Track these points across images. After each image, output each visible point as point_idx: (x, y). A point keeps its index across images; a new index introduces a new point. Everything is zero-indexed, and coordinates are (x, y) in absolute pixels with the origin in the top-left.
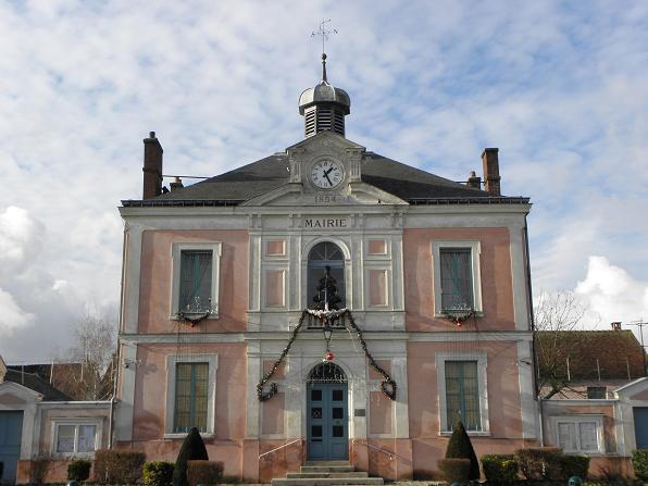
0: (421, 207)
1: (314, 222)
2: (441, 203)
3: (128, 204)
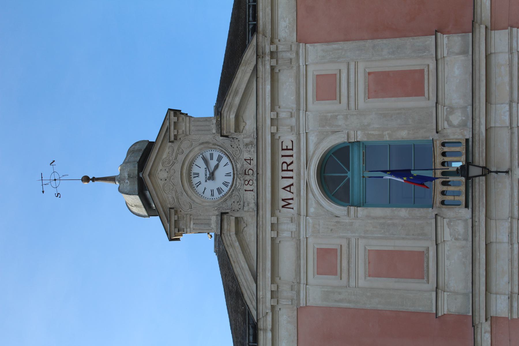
0: (261, 14)
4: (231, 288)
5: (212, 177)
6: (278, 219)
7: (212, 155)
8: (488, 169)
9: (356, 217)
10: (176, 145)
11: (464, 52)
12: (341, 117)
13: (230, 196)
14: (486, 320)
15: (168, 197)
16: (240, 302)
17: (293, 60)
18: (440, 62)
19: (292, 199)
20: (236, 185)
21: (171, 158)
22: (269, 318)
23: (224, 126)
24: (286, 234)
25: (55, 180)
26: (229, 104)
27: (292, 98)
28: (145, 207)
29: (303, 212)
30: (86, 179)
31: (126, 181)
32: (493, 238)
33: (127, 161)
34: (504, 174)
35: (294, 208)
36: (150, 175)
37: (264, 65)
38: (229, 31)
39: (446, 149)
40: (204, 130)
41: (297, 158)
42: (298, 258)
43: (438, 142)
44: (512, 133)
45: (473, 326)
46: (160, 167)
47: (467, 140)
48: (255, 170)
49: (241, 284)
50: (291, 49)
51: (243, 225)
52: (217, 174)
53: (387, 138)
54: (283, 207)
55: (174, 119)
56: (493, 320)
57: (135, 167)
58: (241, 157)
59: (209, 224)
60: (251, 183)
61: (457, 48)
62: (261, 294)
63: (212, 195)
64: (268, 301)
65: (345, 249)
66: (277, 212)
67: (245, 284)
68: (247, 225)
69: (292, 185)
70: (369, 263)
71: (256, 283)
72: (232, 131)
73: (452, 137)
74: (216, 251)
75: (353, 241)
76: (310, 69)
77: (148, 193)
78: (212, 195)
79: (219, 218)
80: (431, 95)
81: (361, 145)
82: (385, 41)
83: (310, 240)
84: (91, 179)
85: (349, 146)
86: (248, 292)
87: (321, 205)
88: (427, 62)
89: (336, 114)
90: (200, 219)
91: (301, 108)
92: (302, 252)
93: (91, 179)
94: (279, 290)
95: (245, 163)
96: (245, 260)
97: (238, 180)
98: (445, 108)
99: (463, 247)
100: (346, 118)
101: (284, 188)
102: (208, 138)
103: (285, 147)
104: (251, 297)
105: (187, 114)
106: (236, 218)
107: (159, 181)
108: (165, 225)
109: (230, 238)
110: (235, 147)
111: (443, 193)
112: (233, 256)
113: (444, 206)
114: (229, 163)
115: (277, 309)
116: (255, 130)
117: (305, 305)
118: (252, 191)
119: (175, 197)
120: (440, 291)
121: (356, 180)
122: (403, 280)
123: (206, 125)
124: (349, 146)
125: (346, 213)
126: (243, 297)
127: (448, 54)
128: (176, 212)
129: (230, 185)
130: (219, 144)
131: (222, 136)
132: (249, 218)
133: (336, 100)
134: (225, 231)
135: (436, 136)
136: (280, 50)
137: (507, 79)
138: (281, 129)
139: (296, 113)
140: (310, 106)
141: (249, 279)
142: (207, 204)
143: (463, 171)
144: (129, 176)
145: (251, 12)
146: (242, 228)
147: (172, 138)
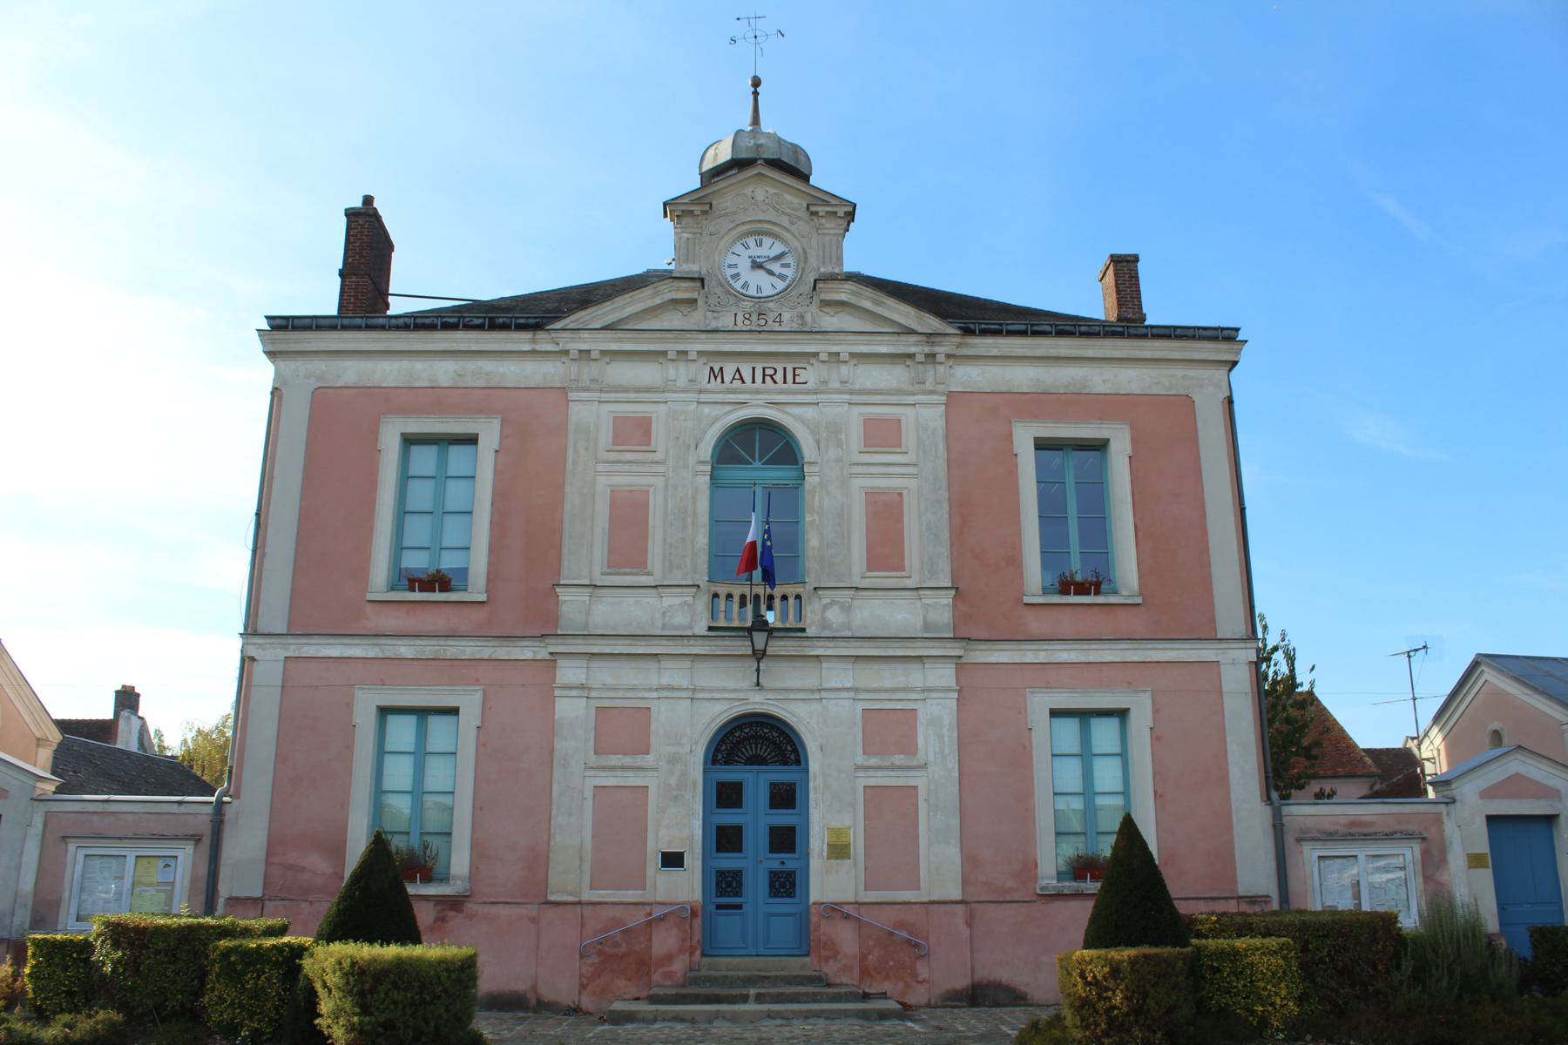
2: (1035, 334)
3: (281, 325)
4: (596, 292)
5: (757, 265)
6: (694, 360)
7: (787, 266)
8: (762, 658)
9: (696, 474)
10: (803, 214)
11: (927, 626)
12: (840, 454)
13: (728, 293)
14: (551, 654)
16: (575, 306)
18: (914, 593)
19: (723, 382)
20: (744, 300)
21: (784, 206)
22: (550, 347)
23: (830, 285)
25: (756, 37)
26: (862, 292)
28: (714, 168)
29: (704, 397)
30: (756, 83)
31: (752, 141)
32: (665, 664)
33: (783, 143)
34: (756, 680)
35: (709, 385)
36: (760, 174)
38: (966, 296)
39: (791, 600)
42: (638, 390)
43: (802, 590)
44: (812, 691)
45: (543, 635)
46: (772, 191)
47: (803, 630)
48: (765, 328)
49: (600, 306)
51: (685, 309)
52: (761, 273)
53: (808, 518)
54: (712, 368)
55: (841, 211)
56: (551, 662)
57: (773, 154)
58: (784, 309)
59: (687, 261)
60: (747, 322)
61: (933, 617)
62: (586, 335)
63: (730, 266)
64: (575, 344)
65: (650, 456)
66: (704, 360)
67: (600, 312)
68: (686, 316)
69: (743, 382)
70: (631, 491)
71: (602, 329)
72: (823, 296)
73: (808, 609)
74: (648, 271)
75: (661, 469)
76: (909, 411)
77: (734, 172)
78: (730, 266)
79: (696, 276)
80: (868, 580)
81: (798, 482)
82: (946, 516)
83: (663, 407)
84: (756, 90)
85: (797, 464)
86: (589, 317)
87: (713, 423)
89: (844, 447)
91: (853, 397)
92: (646, 395)
93: (756, 90)
94: (592, 362)
95: (776, 314)
97: (751, 304)
98: (850, 600)
99: (653, 623)
100: (839, 461)
101: (738, 370)
103: (797, 372)
104: (581, 321)
105: (848, 231)
106: (695, 301)
107: (751, 190)
108: (687, 196)
109: (668, 292)
110: (799, 301)
112: (640, 296)
113: (711, 597)
114: (776, 291)
115: (564, 359)
116: (823, 329)
117: (569, 398)
118: (735, 324)
119: (727, 211)
120: (591, 590)
121: (748, 474)
122: (606, 538)
123: (831, 259)
124: (797, 464)
125: (702, 459)
126: (582, 309)
127: (925, 604)
128: (705, 213)
129: (744, 292)
130: (804, 276)
131: (815, 280)
132: (696, 319)
133: (865, 446)
134: (677, 284)
135: (809, 587)
136: (938, 367)
137: (888, 684)
138: (824, 367)
140: (856, 410)
141: (607, 318)
142: (717, 258)
143: (760, 624)
144: (759, 146)
145: (993, 327)
146: (682, 309)
147: (813, 209)
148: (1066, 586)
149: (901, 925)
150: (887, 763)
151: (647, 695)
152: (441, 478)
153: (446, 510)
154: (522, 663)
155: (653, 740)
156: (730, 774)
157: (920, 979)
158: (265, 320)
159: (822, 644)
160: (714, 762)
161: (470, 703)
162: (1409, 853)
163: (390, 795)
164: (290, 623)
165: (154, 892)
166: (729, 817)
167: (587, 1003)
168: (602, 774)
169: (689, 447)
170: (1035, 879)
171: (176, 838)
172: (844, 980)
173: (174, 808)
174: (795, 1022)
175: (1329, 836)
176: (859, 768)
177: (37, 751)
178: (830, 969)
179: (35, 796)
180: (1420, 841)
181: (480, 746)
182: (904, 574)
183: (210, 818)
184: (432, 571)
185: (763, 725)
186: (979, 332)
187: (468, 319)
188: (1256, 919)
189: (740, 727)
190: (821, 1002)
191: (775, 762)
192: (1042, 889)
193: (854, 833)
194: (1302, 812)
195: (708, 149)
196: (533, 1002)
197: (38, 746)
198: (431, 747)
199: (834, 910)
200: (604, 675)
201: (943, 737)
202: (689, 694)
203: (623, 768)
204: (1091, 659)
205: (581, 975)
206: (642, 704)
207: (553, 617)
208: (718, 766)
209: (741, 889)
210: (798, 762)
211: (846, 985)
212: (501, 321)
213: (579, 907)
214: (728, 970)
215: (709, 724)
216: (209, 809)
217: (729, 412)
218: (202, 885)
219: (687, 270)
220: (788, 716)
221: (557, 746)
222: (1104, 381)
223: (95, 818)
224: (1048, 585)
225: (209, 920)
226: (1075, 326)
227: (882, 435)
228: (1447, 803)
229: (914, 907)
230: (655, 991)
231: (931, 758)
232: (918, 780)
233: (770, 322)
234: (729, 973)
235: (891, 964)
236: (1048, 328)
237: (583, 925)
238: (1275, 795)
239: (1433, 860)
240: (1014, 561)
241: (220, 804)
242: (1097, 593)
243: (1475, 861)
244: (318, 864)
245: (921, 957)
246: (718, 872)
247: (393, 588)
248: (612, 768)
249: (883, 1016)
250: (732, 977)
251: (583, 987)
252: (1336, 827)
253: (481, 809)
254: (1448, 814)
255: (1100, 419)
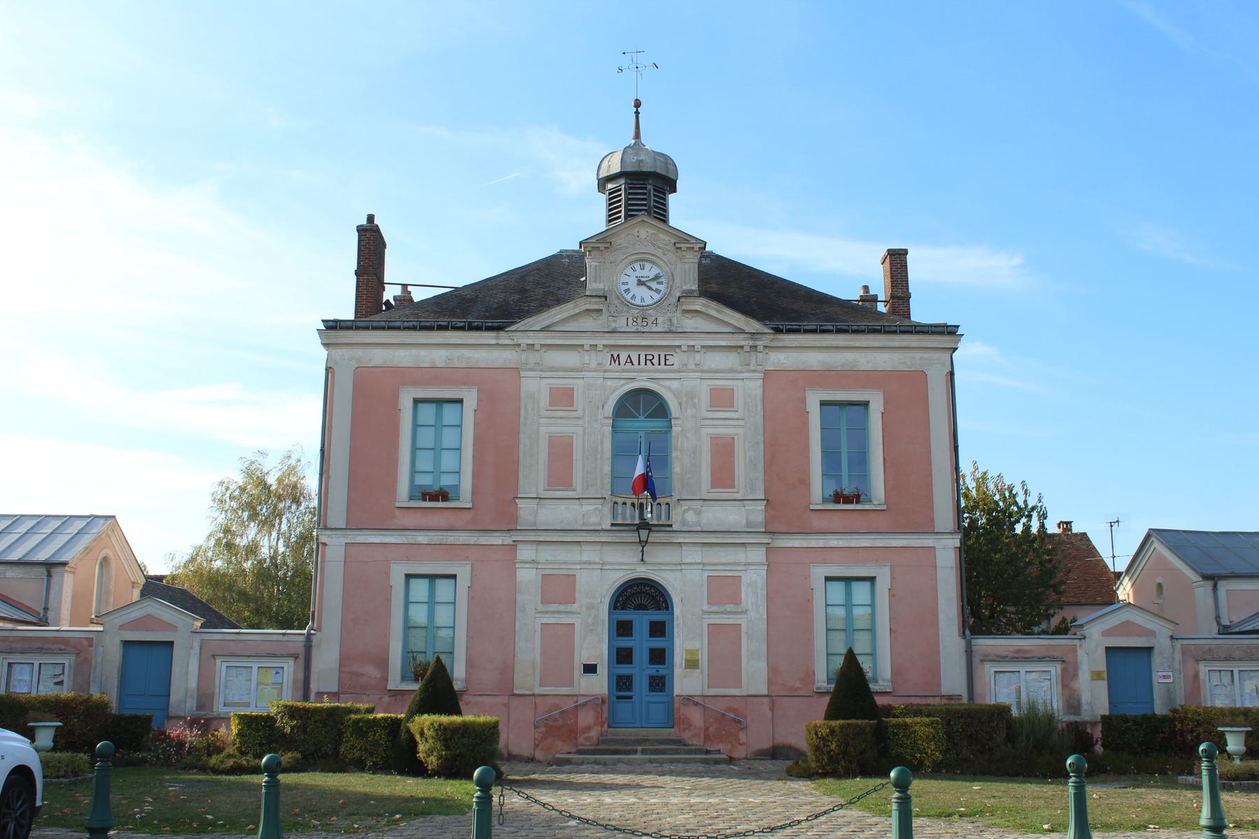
0: (792, 337)
1: (623, 358)
3: (333, 326)
5: (640, 283)
7: (661, 283)
9: (602, 425)
10: (671, 247)
11: (748, 524)
14: (514, 541)
15: (621, 239)
17: (748, 367)
19: (619, 364)
22: (508, 342)
23: (689, 300)
24: (587, 359)
27: (713, 365)
29: (608, 375)
32: (584, 547)
36: (643, 221)
37: (744, 339)
40: (685, 278)
41: (657, 369)
42: (565, 370)
44: (676, 565)
45: (508, 530)
46: (651, 231)
50: (758, 365)
52: (644, 288)
53: (674, 454)
54: (612, 355)
61: (752, 518)
62: (531, 334)
63: (623, 283)
64: (525, 340)
65: (574, 414)
66: (607, 350)
69: (633, 364)
70: (562, 437)
72: (684, 307)
73: (674, 512)
75: (581, 422)
76: (739, 383)
78: (623, 283)
81: (668, 429)
82: (762, 453)
83: (581, 381)
88: (741, 491)
90: (600, 272)
92: (571, 373)
95: (654, 318)
96: (562, 318)
100: (694, 417)
101: (629, 356)
102: (678, 281)
104: (529, 324)
106: (602, 310)
111: (625, 503)
115: (517, 349)
120: (537, 500)
121: (637, 424)
123: (690, 280)
125: (607, 416)
129: (633, 302)
131: (679, 297)
135: (675, 499)
136: (758, 354)
137: (723, 560)
139: (699, 368)
140: (705, 382)
142: (615, 279)
145: (795, 327)
147: (678, 245)
148: (838, 497)
149: (730, 709)
150: (723, 610)
151: (574, 567)
152: (438, 426)
153: (443, 447)
154: (495, 547)
155: (577, 595)
156: (625, 616)
157: (741, 742)
158: (322, 323)
159: (682, 535)
160: (615, 608)
161: (464, 572)
162: (1055, 669)
163: (412, 630)
164: (347, 523)
165: (270, 689)
166: (624, 642)
167: (539, 755)
168: (546, 616)
169: (598, 408)
170: (813, 683)
171: (282, 656)
172: (695, 742)
173: (281, 638)
174: (665, 765)
175: (1002, 659)
176: (705, 612)
177: (132, 591)
178: (686, 736)
179: (193, 630)
180: (1060, 662)
181: (471, 598)
182: (734, 490)
183: (303, 644)
184: (437, 488)
185: (645, 585)
186: (786, 331)
187: (454, 323)
188: (923, 708)
189: (631, 587)
190: (680, 754)
191: (653, 608)
192: (817, 688)
193: (702, 652)
194: (985, 644)
195: (603, 159)
196: (506, 755)
197: (133, 587)
198: (438, 599)
199: (689, 700)
200: (546, 554)
201: (757, 594)
202: (600, 566)
203: (559, 612)
204: (852, 545)
205: (535, 739)
206: (571, 572)
207: (515, 519)
208: (618, 611)
209: (632, 687)
210: (667, 608)
211: (696, 745)
212: (476, 324)
213: (533, 698)
214: (624, 736)
215: (612, 585)
216: (302, 638)
217: (624, 385)
218: (301, 684)
219: (595, 287)
220: (662, 580)
221: (519, 598)
222: (868, 362)
223: (232, 643)
224: (827, 495)
225: (308, 705)
226: (848, 326)
227: (722, 399)
228: (1080, 639)
229: (738, 698)
230: (580, 747)
231: (750, 607)
232: (741, 620)
233: (650, 324)
234: (625, 738)
235: (724, 733)
236: (831, 328)
237: (536, 708)
238: (968, 632)
239: (1069, 674)
240: (805, 482)
241: (309, 635)
242: (858, 502)
243: (1096, 676)
244: (372, 672)
245: (742, 729)
246: (617, 676)
247: (411, 499)
248: (553, 612)
249: (717, 762)
250: (627, 739)
251: (536, 746)
252: (1007, 653)
253: (472, 638)
254: (1080, 646)
255: (864, 387)
